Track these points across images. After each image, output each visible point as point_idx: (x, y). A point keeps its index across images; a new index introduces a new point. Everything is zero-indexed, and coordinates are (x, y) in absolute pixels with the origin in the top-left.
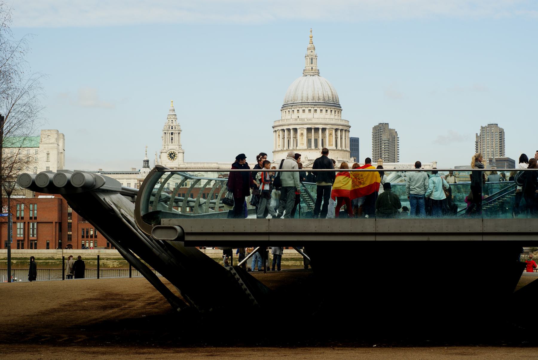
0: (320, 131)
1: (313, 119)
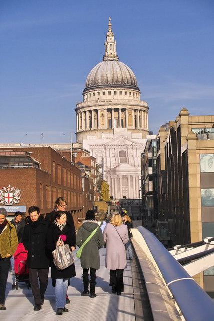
1: (113, 101)
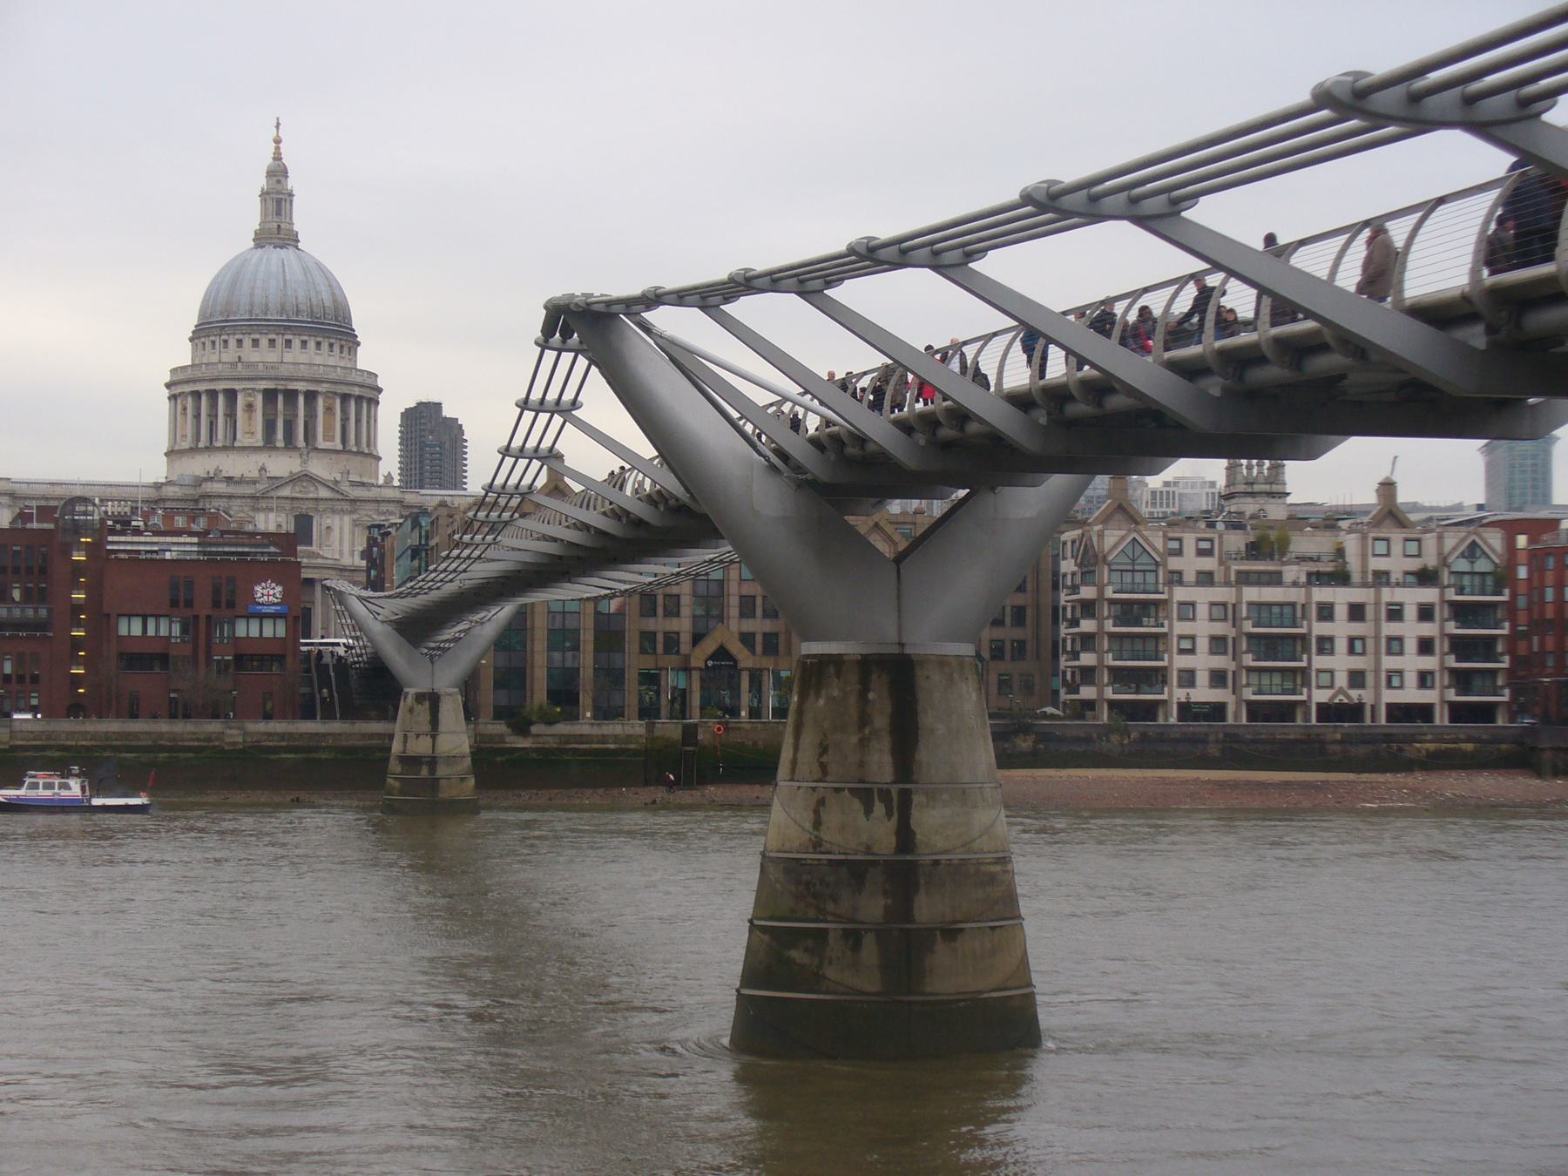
0: (301, 399)
